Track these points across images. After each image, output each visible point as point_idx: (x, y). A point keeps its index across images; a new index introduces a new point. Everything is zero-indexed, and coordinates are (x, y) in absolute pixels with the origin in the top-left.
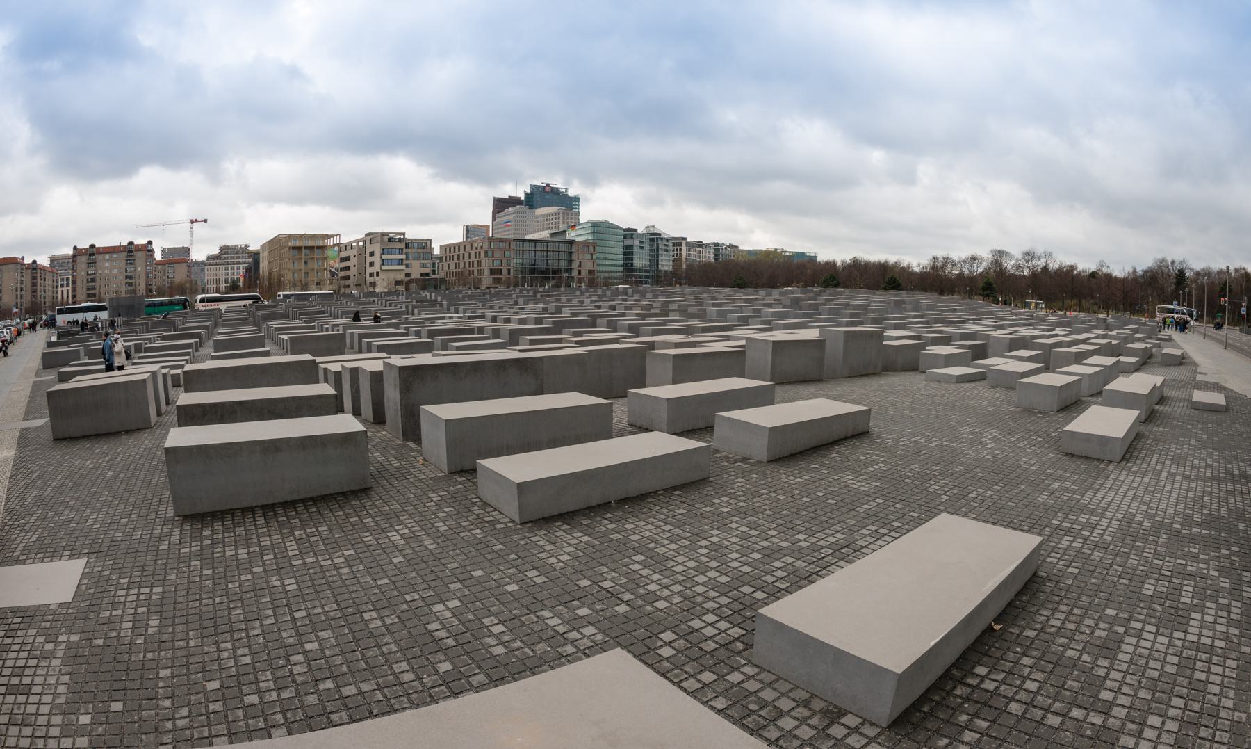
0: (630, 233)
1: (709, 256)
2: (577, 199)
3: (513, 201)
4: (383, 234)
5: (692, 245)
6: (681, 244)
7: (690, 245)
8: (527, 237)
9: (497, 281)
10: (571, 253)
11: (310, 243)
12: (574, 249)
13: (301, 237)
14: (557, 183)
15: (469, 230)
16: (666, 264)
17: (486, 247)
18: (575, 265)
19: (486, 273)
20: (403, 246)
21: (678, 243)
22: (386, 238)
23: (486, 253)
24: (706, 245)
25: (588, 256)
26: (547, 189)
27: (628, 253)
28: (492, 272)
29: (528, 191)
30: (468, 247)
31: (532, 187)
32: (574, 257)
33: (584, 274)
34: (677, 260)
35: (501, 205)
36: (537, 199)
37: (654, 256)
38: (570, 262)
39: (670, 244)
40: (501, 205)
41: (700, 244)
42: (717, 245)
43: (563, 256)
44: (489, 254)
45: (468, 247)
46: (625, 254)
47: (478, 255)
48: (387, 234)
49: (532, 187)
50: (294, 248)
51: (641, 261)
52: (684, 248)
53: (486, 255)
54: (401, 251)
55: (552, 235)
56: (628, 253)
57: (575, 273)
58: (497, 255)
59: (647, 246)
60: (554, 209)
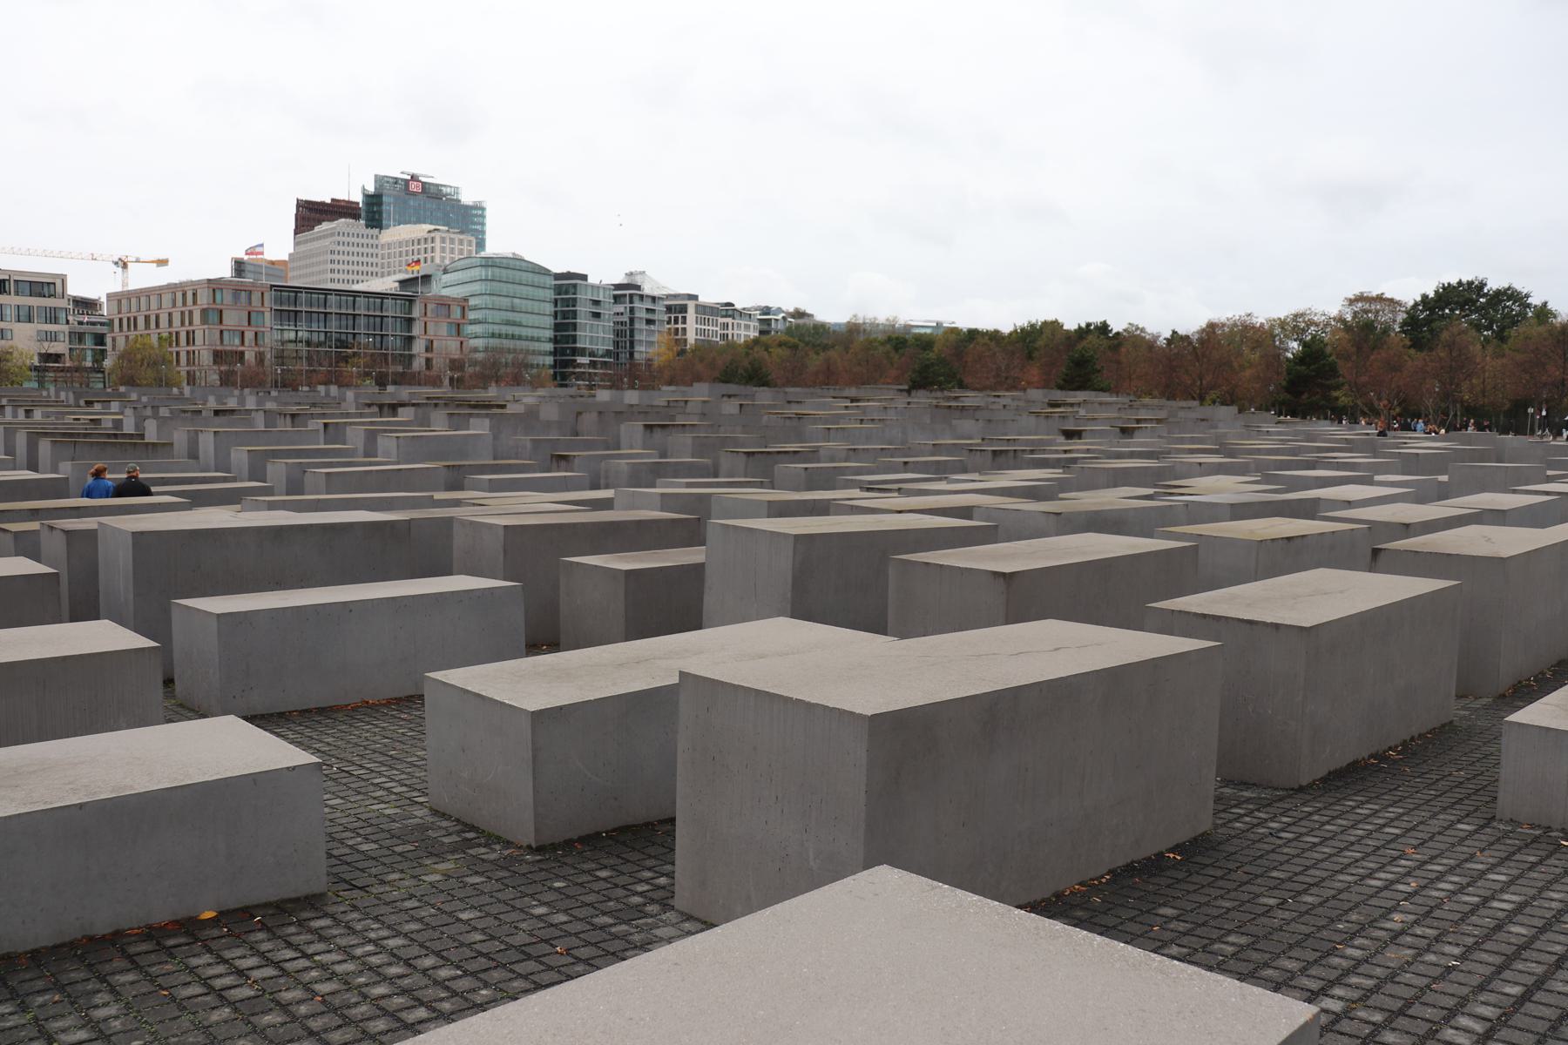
0: (567, 286)
1: (744, 332)
5: (707, 311)
6: (684, 309)
8: (356, 287)
9: (227, 380)
12: (417, 312)
14: (435, 171)
15: (239, 266)
17: (204, 299)
18: (418, 347)
19: (206, 358)
21: (677, 308)
23: (204, 312)
24: (741, 314)
25: (443, 329)
26: (414, 187)
27: (565, 325)
28: (218, 356)
31: (379, 180)
32: (417, 330)
33: (438, 363)
38: (409, 340)
39: (660, 307)
40: (311, 214)
41: (728, 310)
42: (766, 310)
44: (214, 315)
45: (167, 299)
46: (557, 327)
47: (187, 318)
49: (379, 180)
51: (594, 336)
52: (691, 315)
53: (204, 320)
55: (403, 283)
56: (565, 325)
57: (418, 364)
58: (233, 319)
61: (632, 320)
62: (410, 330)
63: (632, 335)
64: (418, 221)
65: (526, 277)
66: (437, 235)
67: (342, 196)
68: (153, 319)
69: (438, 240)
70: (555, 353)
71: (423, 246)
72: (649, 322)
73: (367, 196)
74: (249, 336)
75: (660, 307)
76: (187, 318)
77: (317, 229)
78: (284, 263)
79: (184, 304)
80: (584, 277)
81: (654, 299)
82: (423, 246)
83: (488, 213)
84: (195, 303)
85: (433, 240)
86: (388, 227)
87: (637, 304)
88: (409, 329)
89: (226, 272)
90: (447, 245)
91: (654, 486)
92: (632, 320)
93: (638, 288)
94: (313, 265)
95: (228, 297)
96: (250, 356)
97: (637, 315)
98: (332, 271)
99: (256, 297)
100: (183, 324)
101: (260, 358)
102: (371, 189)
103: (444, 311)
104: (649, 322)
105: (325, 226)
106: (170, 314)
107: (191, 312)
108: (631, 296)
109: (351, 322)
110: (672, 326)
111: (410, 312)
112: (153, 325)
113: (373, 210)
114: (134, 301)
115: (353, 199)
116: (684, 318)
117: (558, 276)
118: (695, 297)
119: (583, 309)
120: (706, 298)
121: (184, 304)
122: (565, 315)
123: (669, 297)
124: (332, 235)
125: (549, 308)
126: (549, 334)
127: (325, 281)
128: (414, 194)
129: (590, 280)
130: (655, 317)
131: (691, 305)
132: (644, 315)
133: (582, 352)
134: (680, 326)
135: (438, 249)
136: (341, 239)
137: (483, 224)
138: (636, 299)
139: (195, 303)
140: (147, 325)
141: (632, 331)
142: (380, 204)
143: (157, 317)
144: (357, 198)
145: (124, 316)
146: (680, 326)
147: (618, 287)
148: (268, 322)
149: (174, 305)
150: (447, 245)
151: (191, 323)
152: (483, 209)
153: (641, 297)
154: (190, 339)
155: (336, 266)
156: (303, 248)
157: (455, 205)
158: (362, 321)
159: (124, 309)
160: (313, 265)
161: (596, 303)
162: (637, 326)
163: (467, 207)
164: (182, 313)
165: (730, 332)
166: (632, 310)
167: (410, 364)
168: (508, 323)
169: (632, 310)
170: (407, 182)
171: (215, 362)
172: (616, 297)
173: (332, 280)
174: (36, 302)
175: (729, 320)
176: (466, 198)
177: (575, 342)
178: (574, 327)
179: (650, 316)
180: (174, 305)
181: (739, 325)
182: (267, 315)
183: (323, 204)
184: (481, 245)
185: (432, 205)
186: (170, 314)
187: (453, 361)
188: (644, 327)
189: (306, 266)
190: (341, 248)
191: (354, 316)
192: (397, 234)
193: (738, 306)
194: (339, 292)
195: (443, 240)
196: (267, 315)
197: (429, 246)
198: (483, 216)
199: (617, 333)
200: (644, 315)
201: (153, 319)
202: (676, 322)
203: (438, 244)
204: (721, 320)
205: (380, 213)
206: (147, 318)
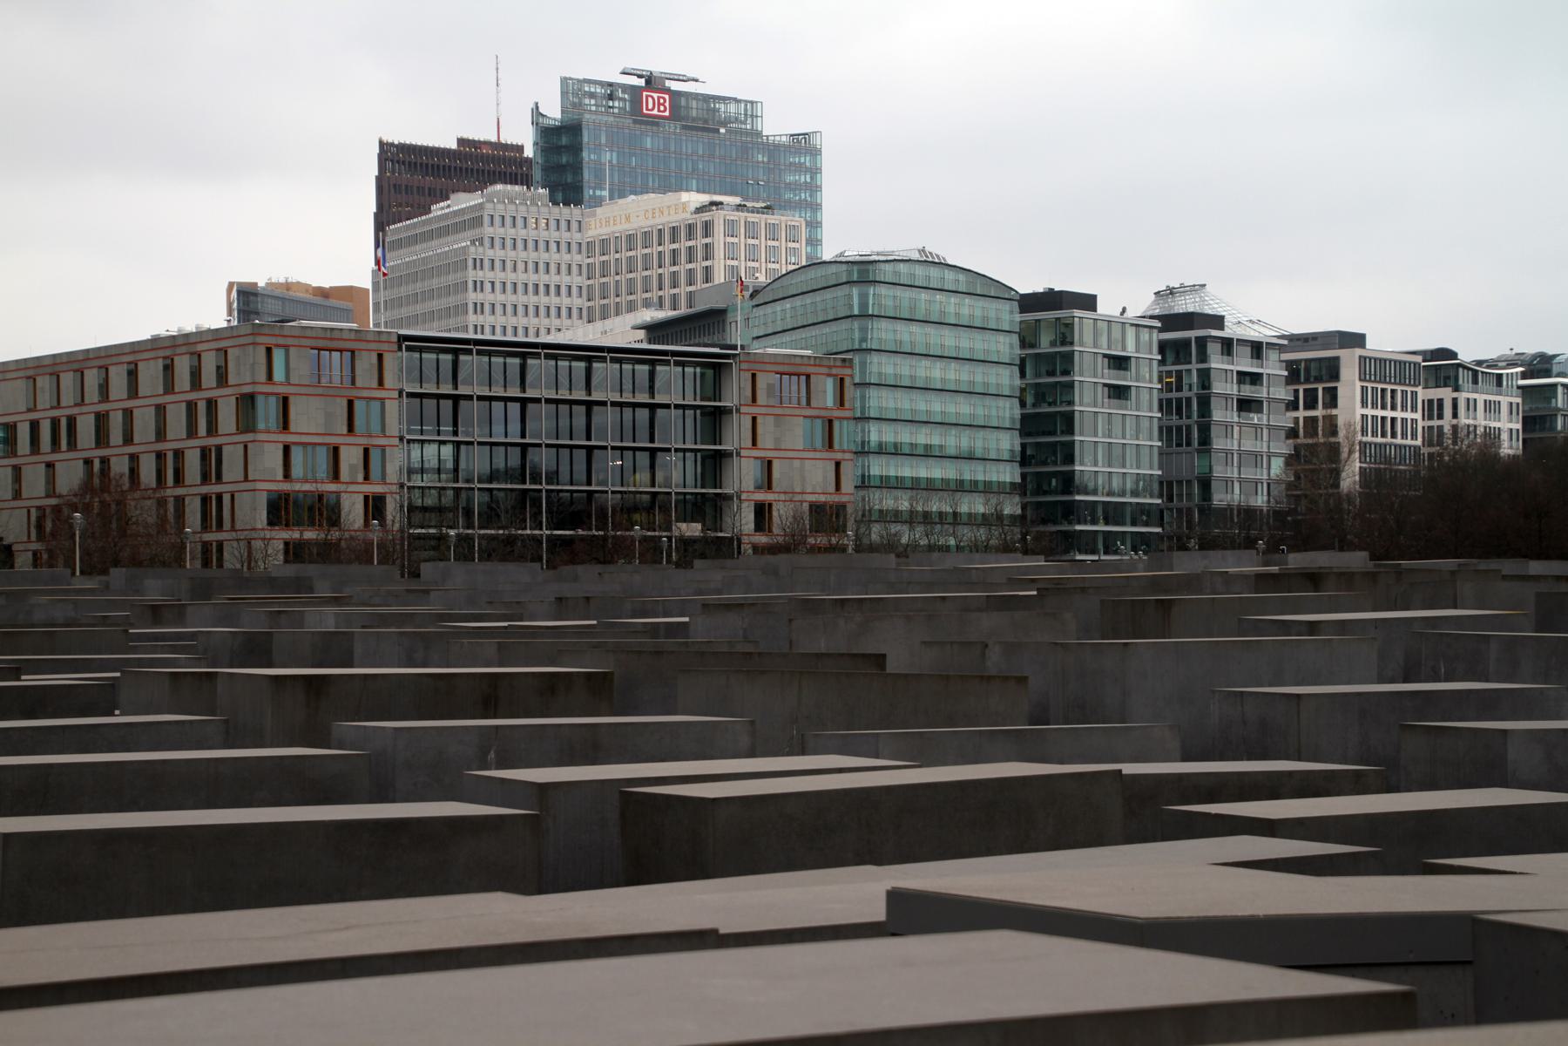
0: (1049, 323)
2: (804, 147)
3: (479, 164)
6: (1331, 370)
7: (1381, 370)
10: (714, 419)
12: (734, 393)
16: (1250, 462)
21: (1315, 364)
23: (247, 402)
24: (1478, 373)
25: (798, 433)
26: (653, 104)
30: (150, 375)
31: (572, 90)
32: (735, 435)
34: (1314, 454)
35: (413, 181)
36: (598, 156)
37: (1186, 423)
38: (714, 463)
39: (1272, 367)
40: (413, 181)
41: (1441, 367)
42: (1540, 365)
43: (678, 433)
45: (150, 375)
46: (1029, 425)
47: (203, 415)
49: (572, 90)
52: (1350, 386)
59: (1146, 379)
61: (1205, 403)
63: (1205, 440)
64: (665, 188)
65: (953, 307)
66: (718, 217)
67: (484, 132)
68: (116, 420)
69: (719, 229)
70: (1019, 488)
71: (683, 244)
72: (1245, 405)
74: (350, 458)
76: (203, 415)
77: (438, 209)
79: (196, 382)
80: (1089, 302)
81: (1257, 349)
82: (683, 244)
83: (827, 162)
84: (222, 377)
85: (708, 229)
86: (598, 202)
87: (1217, 363)
88: (715, 434)
90: (741, 240)
93: (1218, 322)
94: (431, 294)
95: (303, 368)
96: (353, 511)
97: (1218, 387)
99: (366, 362)
100: (192, 432)
101: (375, 506)
102: (553, 111)
103: (794, 387)
104: (1245, 405)
105: (462, 202)
106: (161, 410)
107: (212, 405)
108: (1202, 342)
109: (579, 421)
110: (1302, 414)
111: (717, 396)
112: (116, 436)
113: (560, 162)
114: (67, 380)
115: (508, 138)
116: (1332, 398)
117: (1030, 302)
118: (1357, 340)
119: (1089, 377)
120: (1382, 342)
121: (196, 382)
122: (1041, 393)
125: (1007, 379)
126: (1008, 443)
128: (654, 121)
129: (1106, 308)
130: (1261, 393)
131: (1349, 361)
132: (1232, 389)
134: (1319, 412)
135: (719, 251)
137: (814, 188)
138: (1213, 349)
139: (222, 377)
140: (102, 437)
141: (1205, 430)
142: (576, 149)
143: (72, 421)
144: (523, 137)
145: (45, 419)
146: (1319, 412)
147: (1171, 321)
148: (393, 427)
149: (169, 387)
150: (741, 240)
151: (212, 429)
152: (815, 152)
153: (1227, 345)
154: (212, 463)
157: (751, 140)
158: (606, 419)
159: (45, 399)
160: (431, 294)
161: (1120, 363)
162: (1217, 415)
163: (773, 149)
164: (191, 407)
165: (1447, 422)
166: (1205, 376)
167: (718, 513)
171: (273, 521)
175: (1446, 394)
176: (775, 125)
177: (1070, 459)
178: (1068, 422)
179: (1248, 391)
180: (169, 387)
181: (1471, 405)
182: (392, 407)
185: (694, 145)
186: (161, 410)
187: (816, 509)
188: (1234, 417)
189: (415, 298)
191: (589, 405)
192: (622, 215)
193: (1466, 356)
196: (392, 407)
198: (815, 171)
199: (1166, 432)
200: (1232, 389)
201: (116, 420)
202: (1311, 403)
203: (719, 239)
204: (1423, 394)
205: (577, 168)
206: (101, 420)
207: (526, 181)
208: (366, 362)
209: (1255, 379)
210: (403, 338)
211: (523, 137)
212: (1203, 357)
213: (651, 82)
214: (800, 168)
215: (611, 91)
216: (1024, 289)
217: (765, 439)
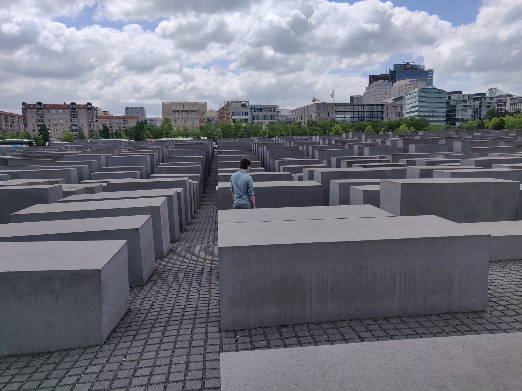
3: (383, 77)
4: (237, 102)
10: (382, 113)
11: (186, 108)
13: (179, 103)
15: (352, 98)
20: (248, 110)
22: (240, 105)
26: (407, 67)
29: (392, 69)
31: (395, 66)
32: (385, 115)
36: (398, 75)
38: (382, 119)
39: (494, 100)
48: (241, 102)
49: (395, 66)
50: (173, 111)
52: (508, 103)
54: (246, 113)
60: (407, 81)
61: (480, 107)
62: (382, 116)
66: (412, 82)
67: (384, 72)
73: (391, 71)
75: (494, 100)
78: (362, 96)
81: (491, 98)
87: (483, 100)
89: (348, 101)
91: (491, 167)
92: (480, 107)
97: (483, 104)
98: (376, 98)
102: (392, 69)
103: (394, 109)
105: (375, 83)
108: (481, 98)
113: (392, 77)
118: (511, 96)
123: (498, 97)
124: (376, 86)
127: (374, 101)
128: (407, 69)
129: (463, 93)
132: (486, 104)
133: (458, 120)
134: (503, 107)
136: (379, 87)
137: (432, 77)
141: (480, 111)
144: (388, 73)
152: (432, 72)
153: (485, 98)
155: (377, 96)
156: (368, 91)
162: (482, 108)
168: (430, 112)
169: (481, 103)
170: (405, 65)
172: (474, 99)
173: (376, 101)
174: (269, 114)
176: (427, 68)
179: (489, 105)
183: (378, 76)
184: (431, 84)
190: (379, 90)
192: (400, 83)
194: (377, 105)
195: (414, 84)
197: (410, 86)
198: (432, 74)
200: (486, 104)
202: (502, 106)
203: (412, 86)
207: (388, 79)
208: (331, 108)
209: (490, 103)
210: (336, 104)
211: (388, 73)
212: (481, 100)
213: (408, 63)
214: (430, 74)
215: (401, 65)
216: (448, 91)
217: (389, 116)
